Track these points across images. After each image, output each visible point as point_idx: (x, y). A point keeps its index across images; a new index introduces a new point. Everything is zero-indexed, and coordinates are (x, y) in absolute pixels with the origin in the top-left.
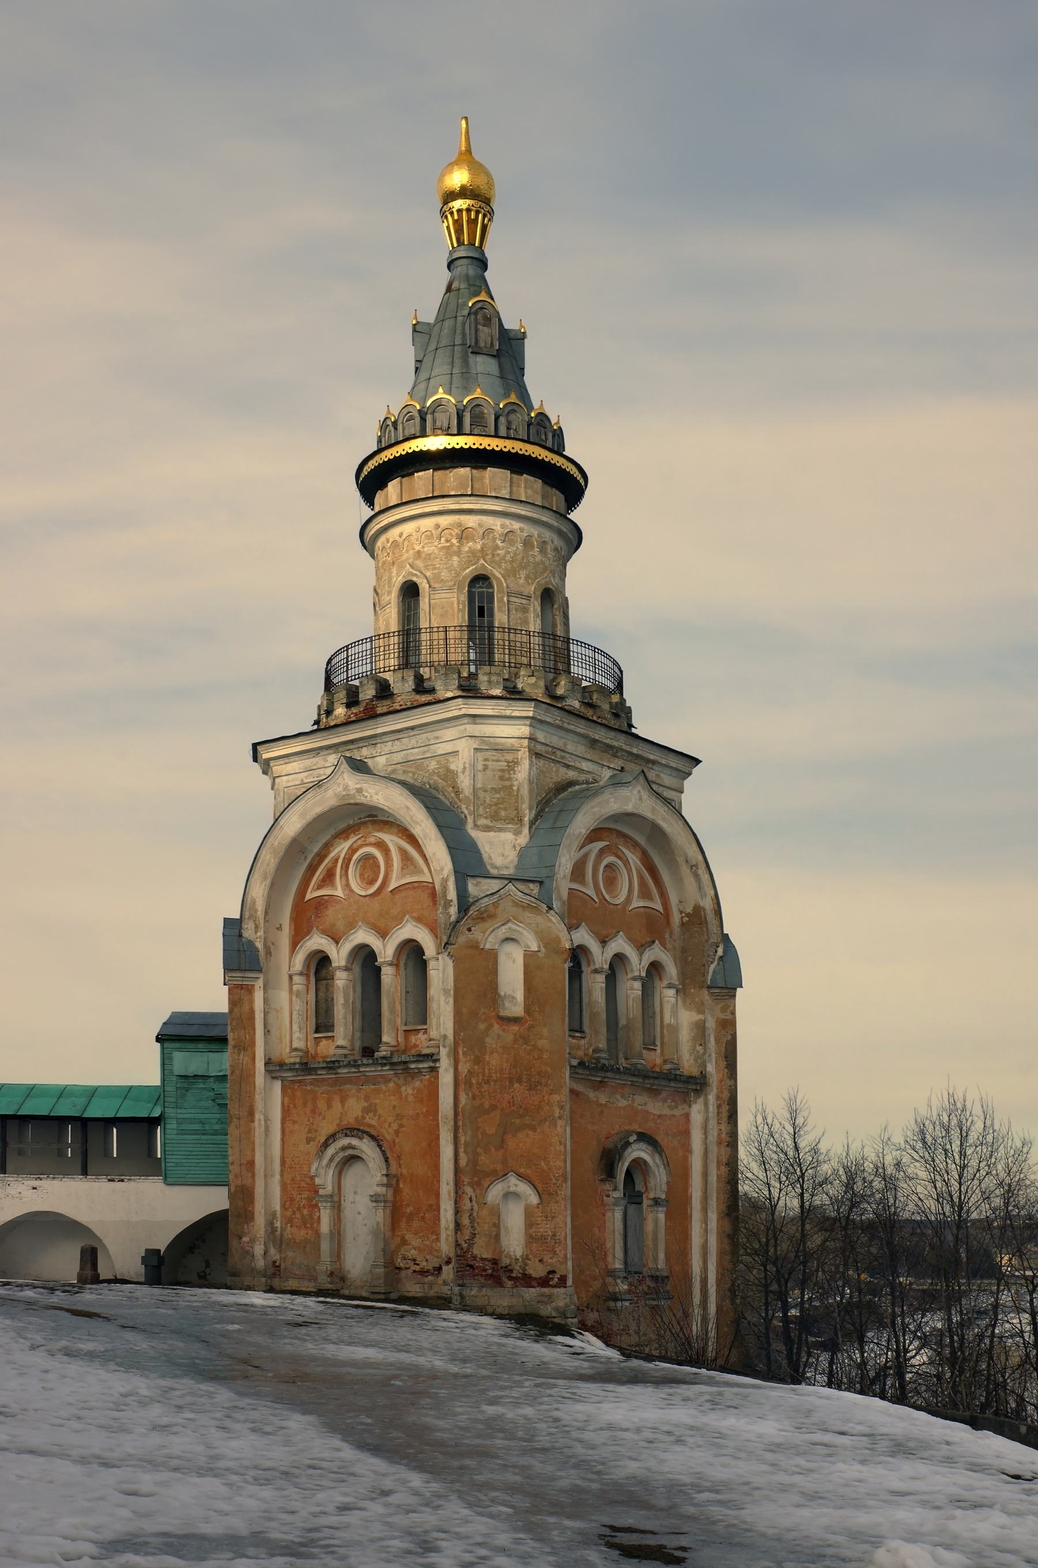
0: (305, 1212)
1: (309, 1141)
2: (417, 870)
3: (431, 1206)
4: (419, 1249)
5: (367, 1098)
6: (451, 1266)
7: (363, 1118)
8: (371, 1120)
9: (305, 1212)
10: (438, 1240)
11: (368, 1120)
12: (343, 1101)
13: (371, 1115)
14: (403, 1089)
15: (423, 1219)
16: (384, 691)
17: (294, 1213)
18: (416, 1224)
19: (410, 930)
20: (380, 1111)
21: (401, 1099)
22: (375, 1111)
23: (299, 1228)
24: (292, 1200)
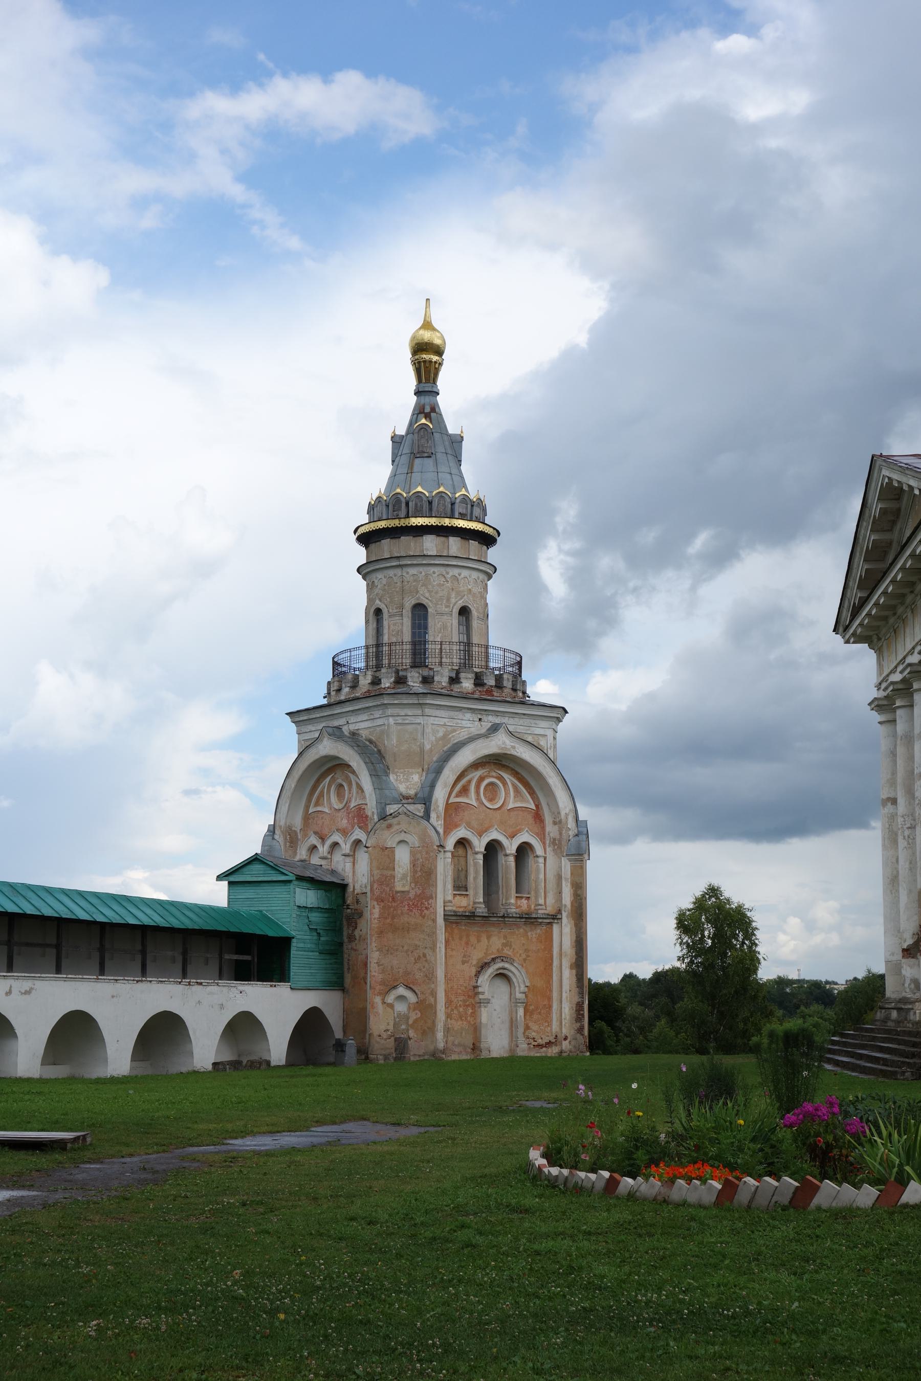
0: (461, 1009)
1: (463, 962)
2: (524, 800)
4: (537, 1032)
5: (505, 937)
6: (567, 1041)
7: (503, 950)
8: (507, 952)
9: (461, 1009)
10: (550, 1025)
11: (505, 951)
12: (489, 938)
14: (529, 934)
15: (540, 1013)
16: (499, 685)
17: (452, 1010)
18: (535, 1017)
19: (524, 837)
20: (514, 946)
21: (528, 939)
23: (457, 1020)
24: (451, 1002)
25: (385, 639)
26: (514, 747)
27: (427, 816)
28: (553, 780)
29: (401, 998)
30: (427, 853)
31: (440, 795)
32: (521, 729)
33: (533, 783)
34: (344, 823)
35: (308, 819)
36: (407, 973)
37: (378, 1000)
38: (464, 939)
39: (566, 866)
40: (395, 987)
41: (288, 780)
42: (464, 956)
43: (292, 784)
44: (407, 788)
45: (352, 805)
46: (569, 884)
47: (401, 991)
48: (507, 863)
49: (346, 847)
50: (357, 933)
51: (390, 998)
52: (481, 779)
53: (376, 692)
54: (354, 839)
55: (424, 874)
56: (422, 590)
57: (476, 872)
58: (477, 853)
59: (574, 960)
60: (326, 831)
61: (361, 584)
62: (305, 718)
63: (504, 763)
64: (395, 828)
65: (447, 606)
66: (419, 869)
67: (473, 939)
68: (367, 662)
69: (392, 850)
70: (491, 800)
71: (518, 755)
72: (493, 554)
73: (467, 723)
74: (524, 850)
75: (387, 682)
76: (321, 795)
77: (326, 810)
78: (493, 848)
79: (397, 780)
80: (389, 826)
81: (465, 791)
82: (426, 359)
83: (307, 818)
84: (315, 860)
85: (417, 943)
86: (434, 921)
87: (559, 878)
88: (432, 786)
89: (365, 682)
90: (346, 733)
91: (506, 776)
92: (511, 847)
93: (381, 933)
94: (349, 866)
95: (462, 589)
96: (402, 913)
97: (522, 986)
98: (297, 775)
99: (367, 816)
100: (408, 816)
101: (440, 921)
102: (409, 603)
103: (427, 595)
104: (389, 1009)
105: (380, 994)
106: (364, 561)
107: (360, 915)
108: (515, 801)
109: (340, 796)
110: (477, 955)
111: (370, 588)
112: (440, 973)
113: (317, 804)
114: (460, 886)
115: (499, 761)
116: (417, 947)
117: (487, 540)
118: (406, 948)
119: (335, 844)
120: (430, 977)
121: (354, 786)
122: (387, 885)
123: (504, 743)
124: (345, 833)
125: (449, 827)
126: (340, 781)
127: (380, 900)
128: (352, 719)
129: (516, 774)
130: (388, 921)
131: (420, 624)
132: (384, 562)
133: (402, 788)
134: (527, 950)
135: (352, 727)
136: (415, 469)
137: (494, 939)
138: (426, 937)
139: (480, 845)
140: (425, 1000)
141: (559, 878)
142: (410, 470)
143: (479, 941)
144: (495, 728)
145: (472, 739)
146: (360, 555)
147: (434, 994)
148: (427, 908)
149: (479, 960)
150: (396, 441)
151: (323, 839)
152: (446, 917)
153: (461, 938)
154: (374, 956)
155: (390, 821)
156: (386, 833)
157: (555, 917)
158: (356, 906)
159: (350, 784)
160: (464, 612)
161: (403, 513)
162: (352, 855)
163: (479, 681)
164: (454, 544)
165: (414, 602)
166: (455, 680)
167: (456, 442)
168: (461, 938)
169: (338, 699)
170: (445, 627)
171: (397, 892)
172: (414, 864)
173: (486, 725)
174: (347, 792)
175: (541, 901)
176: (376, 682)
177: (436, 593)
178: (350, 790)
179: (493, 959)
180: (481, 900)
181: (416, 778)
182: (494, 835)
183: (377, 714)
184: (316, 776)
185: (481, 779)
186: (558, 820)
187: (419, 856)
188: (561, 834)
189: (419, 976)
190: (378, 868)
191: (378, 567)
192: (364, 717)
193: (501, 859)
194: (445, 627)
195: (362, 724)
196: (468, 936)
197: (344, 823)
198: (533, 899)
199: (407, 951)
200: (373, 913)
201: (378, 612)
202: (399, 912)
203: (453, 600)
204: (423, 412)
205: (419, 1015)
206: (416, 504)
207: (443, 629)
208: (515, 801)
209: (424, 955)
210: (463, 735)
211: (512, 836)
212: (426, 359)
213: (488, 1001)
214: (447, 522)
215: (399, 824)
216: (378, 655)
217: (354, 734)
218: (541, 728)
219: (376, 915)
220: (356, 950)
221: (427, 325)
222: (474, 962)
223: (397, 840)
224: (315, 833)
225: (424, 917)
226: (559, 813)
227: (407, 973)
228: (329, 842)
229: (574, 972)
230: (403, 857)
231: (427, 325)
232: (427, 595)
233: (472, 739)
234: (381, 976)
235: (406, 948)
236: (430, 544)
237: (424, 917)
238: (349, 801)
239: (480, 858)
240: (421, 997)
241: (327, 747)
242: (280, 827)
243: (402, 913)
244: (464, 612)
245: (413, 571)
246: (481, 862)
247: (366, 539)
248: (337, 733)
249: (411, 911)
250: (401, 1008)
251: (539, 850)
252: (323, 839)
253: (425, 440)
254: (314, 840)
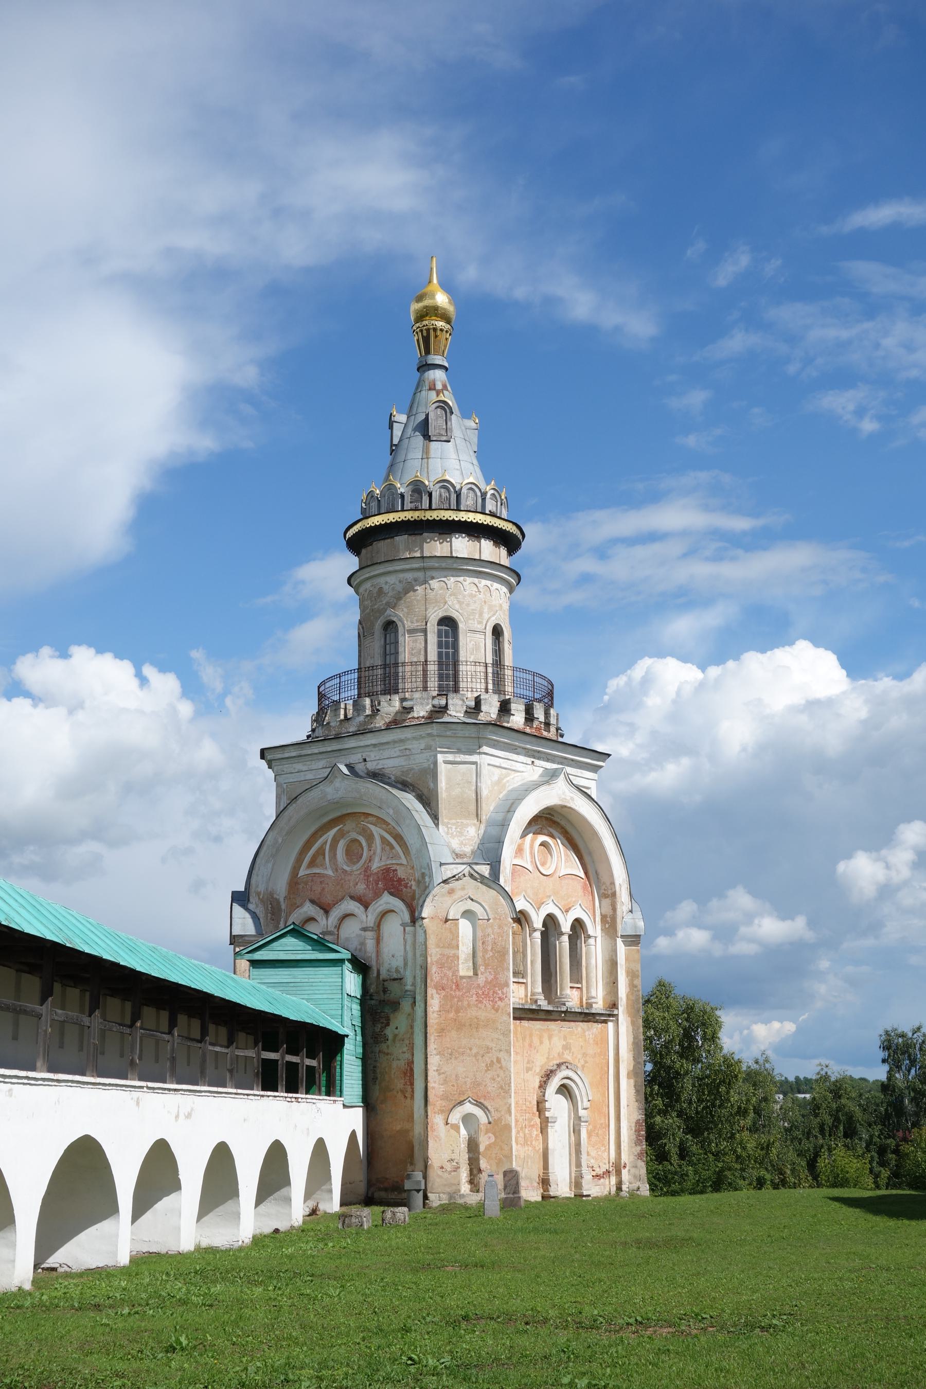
0: (527, 1131)
1: (528, 1070)
3: (601, 1124)
5: (565, 1038)
8: (568, 1057)
9: (527, 1131)
12: (550, 1038)
13: (567, 1051)
14: (587, 1033)
20: (573, 1049)
22: (570, 1049)
26: (572, 799)
30: (500, 927)
35: (297, 883)
36: (476, 1084)
38: (528, 1041)
40: (461, 1103)
41: (271, 833)
42: (528, 1062)
44: (462, 843)
45: (376, 865)
46: (624, 972)
47: (469, 1108)
50: (389, 1032)
51: (455, 1117)
54: (380, 909)
56: (451, 601)
57: (533, 954)
58: (535, 930)
59: (631, 1068)
60: (328, 899)
62: (294, 754)
63: (555, 819)
64: (459, 894)
65: (480, 623)
66: (490, 948)
67: (536, 1040)
68: (359, 688)
71: (576, 808)
76: (321, 852)
77: (330, 872)
79: (448, 833)
80: (451, 892)
83: (294, 883)
85: (491, 1044)
90: (361, 774)
93: (442, 1031)
94: (370, 944)
95: (494, 603)
96: (469, 1005)
97: (585, 1100)
99: (400, 880)
100: (476, 879)
103: (457, 607)
104: (452, 1132)
105: (442, 1111)
107: (395, 1005)
108: (566, 867)
110: (541, 1062)
113: (312, 864)
116: (488, 1050)
118: (474, 1051)
121: (378, 841)
122: (450, 969)
123: (564, 793)
126: (353, 835)
127: (441, 988)
128: (372, 755)
130: (452, 1015)
131: (447, 642)
132: (402, 563)
133: (455, 844)
134: (585, 1055)
135: (371, 766)
136: (432, 453)
137: (555, 1039)
138: (501, 1037)
140: (500, 1119)
143: (541, 1043)
144: (551, 776)
148: (501, 999)
149: (542, 1066)
153: (524, 1039)
154: (434, 1061)
155: (454, 884)
156: (448, 900)
158: (382, 997)
159: (370, 838)
160: (497, 632)
161: (425, 504)
165: (441, 614)
168: (524, 1039)
169: (344, 730)
170: (477, 647)
171: (462, 977)
174: (365, 849)
175: (593, 994)
177: (468, 605)
178: (370, 846)
179: (559, 1065)
180: (540, 990)
182: (550, 908)
186: (610, 892)
187: (489, 930)
188: (614, 909)
189: (492, 1087)
190: (438, 946)
191: (391, 569)
192: (395, 751)
194: (477, 647)
196: (531, 1035)
198: (584, 989)
199: (475, 1056)
200: (435, 1002)
201: (390, 626)
202: (465, 1003)
203: (486, 616)
204: (435, 389)
205: (493, 1139)
206: (440, 495)
208: (566, 867)
209: (499, 1060)
215: (463, 889)
219: (436, 1008)
220: (388, 1054)
222: (538, 1070)
223: (463, 909)
224: (313, 902)
225: (497, 1010)
226: (613, 883)
227: (476, 1084)
228: (336, 913)
229: (632, 1081)
232: (457, 607)
234: (442, 1088)
235: (474, 1051)
237: (497, 1010)
238: (370, 860)
239: (538, 935)
240: (496, 1115)
242: (258, 894)
243: (469, 1005)
244: (497, 632)
246: (539, 941)
249: (481, 1002)
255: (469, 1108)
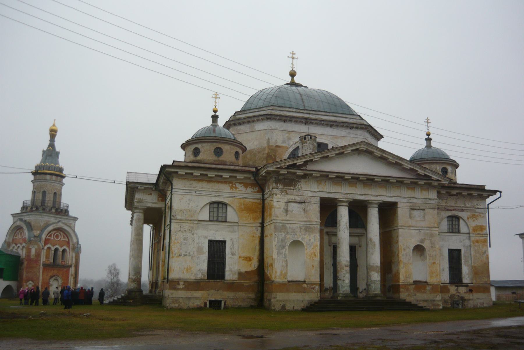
19: (65, 247)
25: (36, 198)
27: (40, 241)
28: (72, 234)
29: (30, 284)
31: (44, 236)
32: (66, 222)
33: (68, 235)
34: (21, 241)
37: (25, 284)
39: (74, 255)
43: (10, 231)
47: (30, 282)
48: (60, 253)
49: (21, 247)
51: (28, 284)
52: (55, 233)
53: (31, 211)
55: (38, 255)
61: (31, 185)
69: (31, 249)
70: (57, 238)
72: (64, 181)
73: (52, 220)
74: (64, 251)
75: (34, 209)
78: (56, 250)
81: (50, 236)
82: (53, 133)
83: (13, 240)
84: (14, 250)
86: (40, 266)
87: (72, 257)
88: (42, 234)
89: (29, 208)
91: (62, 233)
92: (61, 249)
98: (11, 229)
101: (41, 266)
102: (42, 190)
106: (33, 179)
109: (21, 235)
110: (50, 274)
111: (34, 186)
112: (41, 278)
114: (47, 258)
115: (59, 229)
117: (63, 177)
119: (19, 247)
120: (38, 279)
124: (21, 244)
125: (46, 244)
129: (64, 233)
133: (35, 234)
135: (25, 219)
139: (53, 248)
141: (72, 257)
142: (46, 159)
144: (59, 221)
145: (53, 223)
146: (32, 177)
147: (38, 283)
150: (44, 152)
151: (16, 245)
152: (43, 265)
154: (25, 274)
157: (71, 266)
160: (55, 194)
162: (22, 249)
163: (57, 210)
164: (54, 177)
166: (51, 210)
167: (58, 154)
172: (36, 252)
173: (57, 221)
176: (32, 208)
181: (38, 232)
182: (57, 246)
183: (31, 216)
184: (15, 230)
185: (55, 233)
193: (58, 252)
195: (27, 218)
197: (21, 241)
200: (25, 263)
207: (50, 198)
210: (51, 222)
211: (61, 247)
212: (53, 133)
213: (52, 285)
214: (52, 172)
216: (34, 202)
217: (25, 221)
218: (71, 222)
221: (54, 125)
230: (33, 251)
231: (54, 125)
233: (53, 223)
236: (48, 177)
239: (53, 252)
241: (19, 223)
245: (43, 183)
247: (34, 174)
248: (21, 220)
250: (30, 286)
251: (68, 250)
252: (16, 245)
253: (51, 153)
254: (14, 245)
255: (30, 282)
